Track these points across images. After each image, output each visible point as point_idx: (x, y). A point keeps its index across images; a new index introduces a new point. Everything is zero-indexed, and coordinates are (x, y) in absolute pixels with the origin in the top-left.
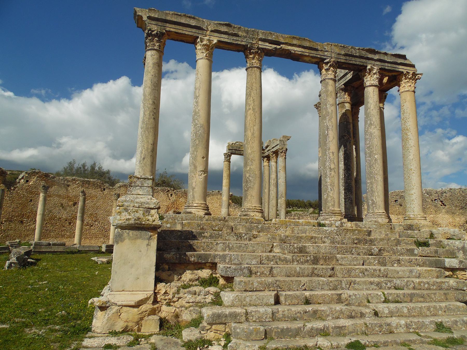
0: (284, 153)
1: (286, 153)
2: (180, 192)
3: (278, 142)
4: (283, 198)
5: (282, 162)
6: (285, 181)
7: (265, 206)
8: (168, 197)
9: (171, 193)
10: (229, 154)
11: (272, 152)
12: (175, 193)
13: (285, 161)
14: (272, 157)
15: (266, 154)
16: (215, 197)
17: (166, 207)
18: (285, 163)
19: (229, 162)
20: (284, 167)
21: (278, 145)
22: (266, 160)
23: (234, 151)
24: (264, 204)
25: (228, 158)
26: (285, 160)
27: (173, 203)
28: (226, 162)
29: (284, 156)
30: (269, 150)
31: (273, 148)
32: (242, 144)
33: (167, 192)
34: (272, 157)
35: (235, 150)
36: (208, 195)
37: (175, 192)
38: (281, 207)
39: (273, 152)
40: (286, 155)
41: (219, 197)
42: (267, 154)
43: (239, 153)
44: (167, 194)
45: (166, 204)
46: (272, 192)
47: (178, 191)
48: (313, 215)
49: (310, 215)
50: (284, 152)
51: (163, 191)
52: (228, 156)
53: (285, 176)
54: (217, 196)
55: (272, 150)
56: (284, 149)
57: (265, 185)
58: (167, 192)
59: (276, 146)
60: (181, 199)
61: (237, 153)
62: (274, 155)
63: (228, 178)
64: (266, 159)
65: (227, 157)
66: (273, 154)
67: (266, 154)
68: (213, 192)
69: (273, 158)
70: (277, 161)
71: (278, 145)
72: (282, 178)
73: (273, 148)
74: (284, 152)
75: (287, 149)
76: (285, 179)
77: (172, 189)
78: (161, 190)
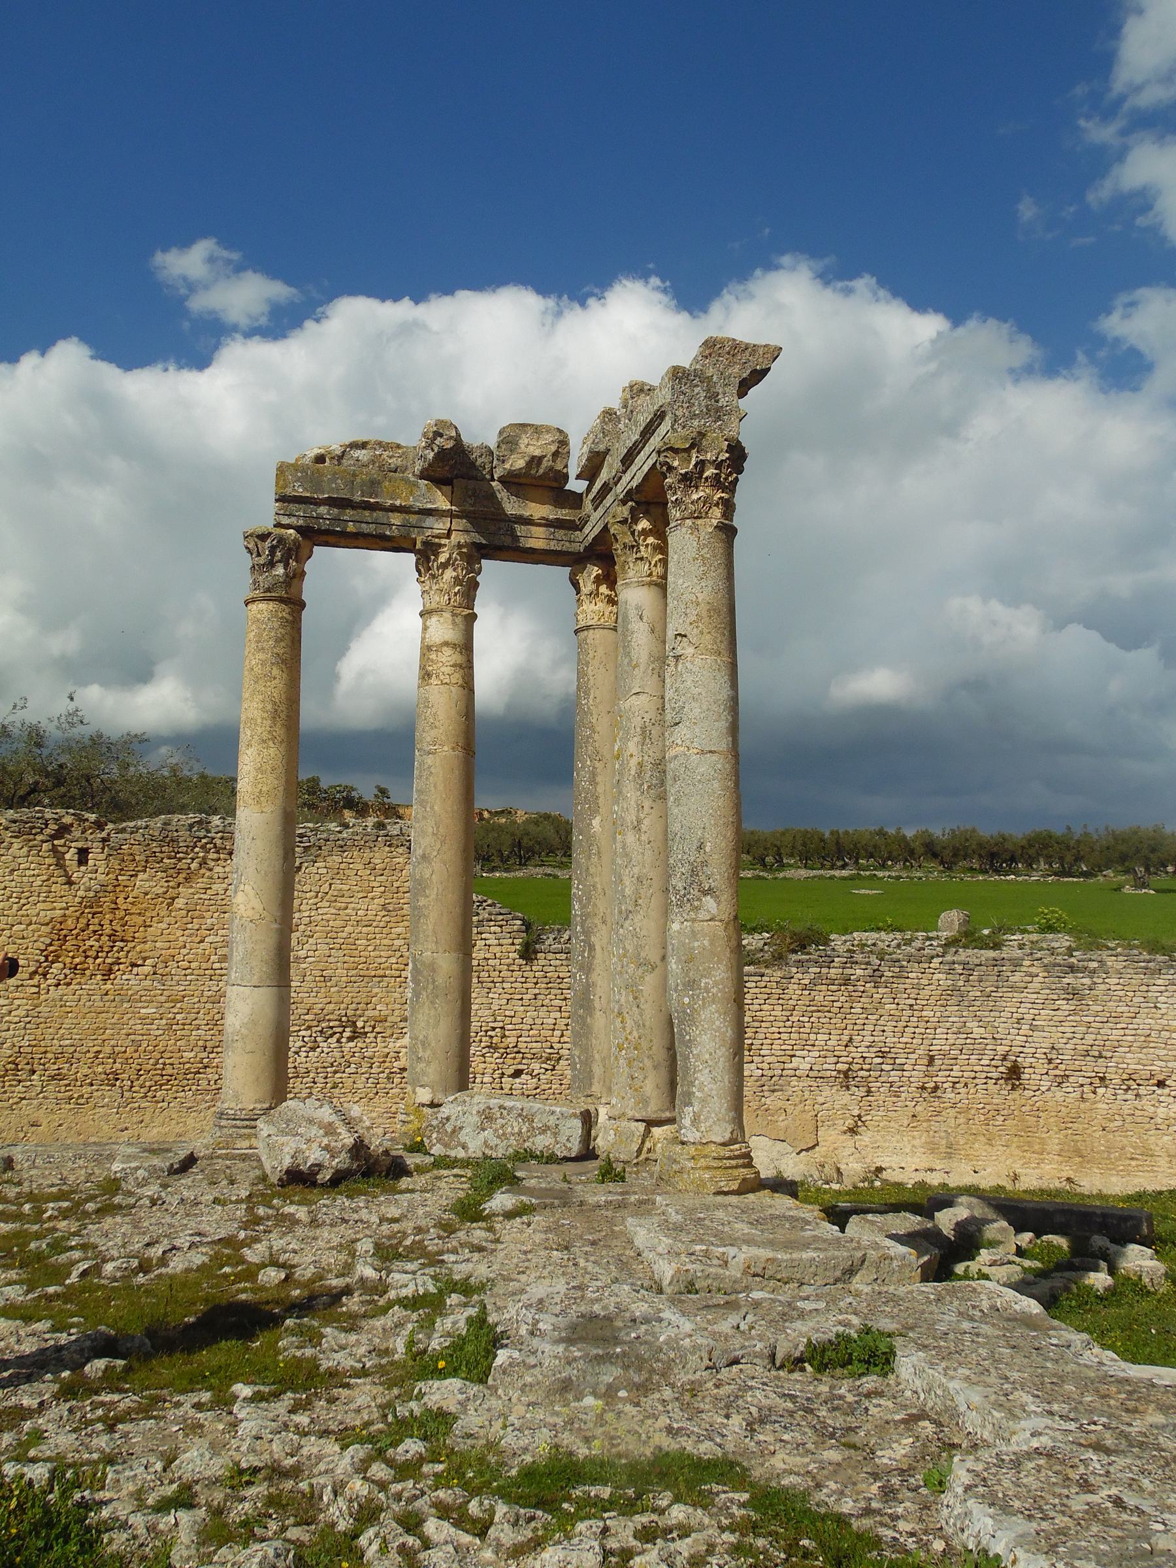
0: (717, 483)
1: (732, 488)
2: (138, 837)
3: (663, 397)
4: (709, 901)
5: (696, 569)
6: (724, 745)
7: (592, 948)
8: (60, 865)
9: (80, 845)
10: (281, 540)
11: (624, 502)
12: (104, 840)
13: (720, 560)
14: (629, 540)
15: (591, 531)
16: (357, 860)
17: (45, 929)
18: (722, 571)
19: (281, 600)
20: (712, 610)
21: (659, 416)
22: (598, 581)
23: (323, 510)
24: (587, 933)
25: (280, 570)
26: (720, 547)
27: (92, 904)
28: (262, 606)
29: (717, 512)
30: (606, 489)
31: (628, 460)
32: (394, 462)
33: (53, 837)
34: (629, 540)
35: (332, 502)
36: (313, 850)
37: (104, 834)
38: (691, 984)
39: (630, 495)
40: (728, 507)
41: (379, 856)
42: (596, 531)
43: (365, 528)
44: (54, 849)
45: (45, 911)
46: (631, 838)
47: (123, 830)
48: (963, 955)
49: (948, 958)
50: (710, 472)
51: (25, 831)
52: (273, 550)
53: (726, 693)
54: (367, 854)
55: (626, 478)
56: (715, 451)
57: (593, 781)
58: (53, 837)
59: (648, 431)
60: (141, 876)
61: (351, 528)
62: (644, 524)
63: (279, 731)
64: (595, 571)
65: (271, 564)
66: (635, 520)
67: (586, 530)
68: (346, 826)
69: (635, 547)
70: (664, 577)
71: (659, 416)
72: (694, 711)
73: (628, 460)
74: (710, 472)
75: (737, 455)
76: (723, 725)
77: (93, 817)
78: (14, 827)
